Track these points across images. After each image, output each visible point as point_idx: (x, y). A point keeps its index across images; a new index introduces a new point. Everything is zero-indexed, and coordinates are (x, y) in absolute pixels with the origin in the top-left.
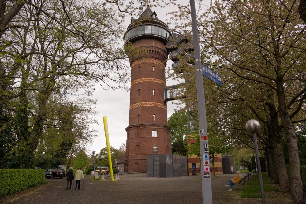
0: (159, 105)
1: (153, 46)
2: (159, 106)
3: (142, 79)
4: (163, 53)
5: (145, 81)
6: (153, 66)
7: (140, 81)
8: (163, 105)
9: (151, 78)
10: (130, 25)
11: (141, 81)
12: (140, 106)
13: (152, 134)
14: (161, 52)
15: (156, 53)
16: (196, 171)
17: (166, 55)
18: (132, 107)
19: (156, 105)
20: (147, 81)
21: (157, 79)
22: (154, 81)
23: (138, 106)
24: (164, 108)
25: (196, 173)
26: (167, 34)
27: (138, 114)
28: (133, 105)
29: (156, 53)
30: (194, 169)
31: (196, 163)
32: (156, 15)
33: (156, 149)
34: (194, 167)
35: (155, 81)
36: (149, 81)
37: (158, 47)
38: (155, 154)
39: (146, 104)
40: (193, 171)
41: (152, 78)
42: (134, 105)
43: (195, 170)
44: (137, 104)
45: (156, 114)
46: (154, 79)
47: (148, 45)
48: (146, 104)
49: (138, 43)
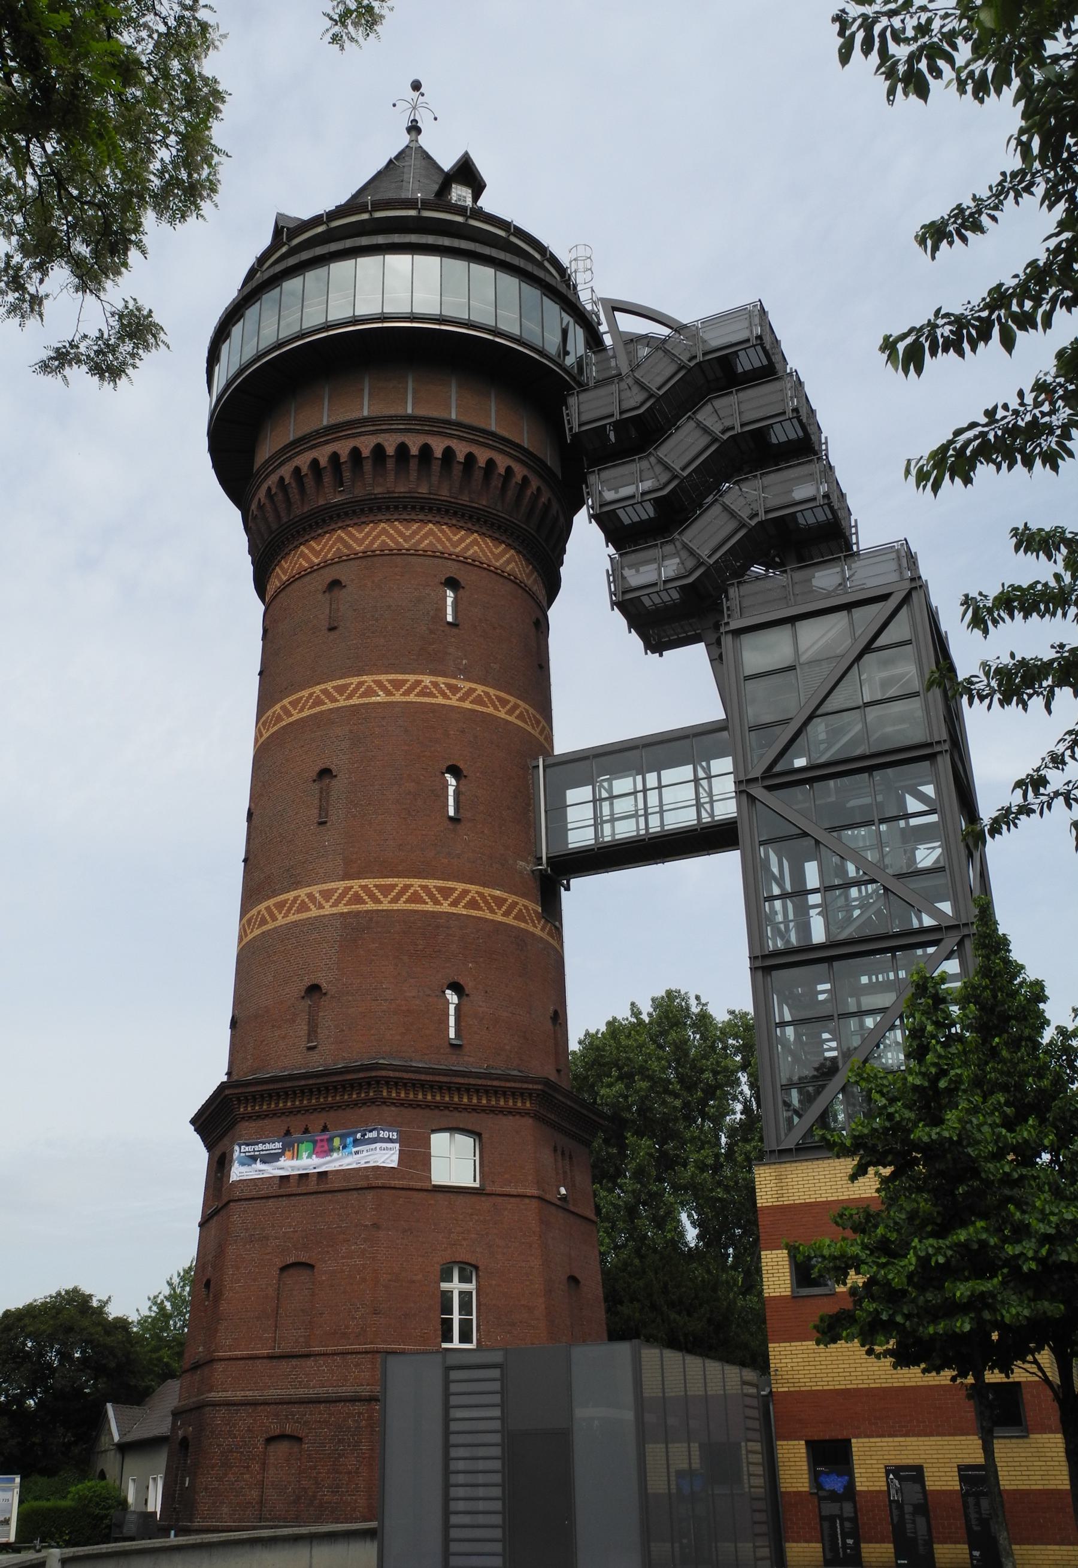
0: (500, 902)
1: (454, 417)
2: (499, 918)
3: (355, 680)
4: (535, 483)
5: (381, 697)
6: (452, 583)
7: (334, 700)
8: (532, 906)
9: (427, 680)
10: (262, 260)
11: (342, 703)
12: (328, 910)
13: (434, 1161)
14: (520, 471)
15: (478, 475)
16: (854, 1520)
17: (555, 506)
18: (264, 922)
19: (473, 904)
20: (398, 697)
21: (480, 689)
22: (454, 702)
23: (314, 912)
24: (538, 931)
25: (857, 1548)
26: (565, 333)
27: (307, 982)
28: (271, 902)
29: (478, 475)
30: (833, 1496)
31: (848, 1442)
32: (477, 186)
33: (465, 1296)
34: (834, 1483)
35: (467, 705)
36: (412, 698)
37: (493, 428)
38: (456, 1344)
39: (386, 890)
40: (831, 1519)
41: (433, 673)
42: (280, 906)
43: (848, 1509)
44: (302, 893)
45: (469, 985)
46: (454, 689)
47: (409, 411)
48: (386, 890)
49: (327, 389)
